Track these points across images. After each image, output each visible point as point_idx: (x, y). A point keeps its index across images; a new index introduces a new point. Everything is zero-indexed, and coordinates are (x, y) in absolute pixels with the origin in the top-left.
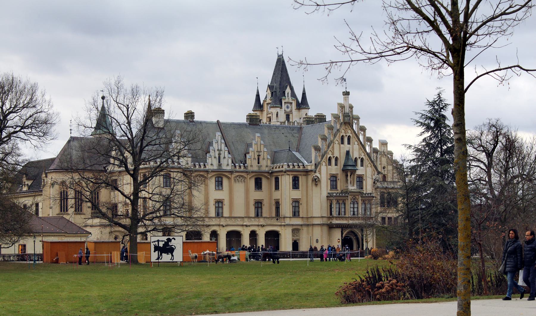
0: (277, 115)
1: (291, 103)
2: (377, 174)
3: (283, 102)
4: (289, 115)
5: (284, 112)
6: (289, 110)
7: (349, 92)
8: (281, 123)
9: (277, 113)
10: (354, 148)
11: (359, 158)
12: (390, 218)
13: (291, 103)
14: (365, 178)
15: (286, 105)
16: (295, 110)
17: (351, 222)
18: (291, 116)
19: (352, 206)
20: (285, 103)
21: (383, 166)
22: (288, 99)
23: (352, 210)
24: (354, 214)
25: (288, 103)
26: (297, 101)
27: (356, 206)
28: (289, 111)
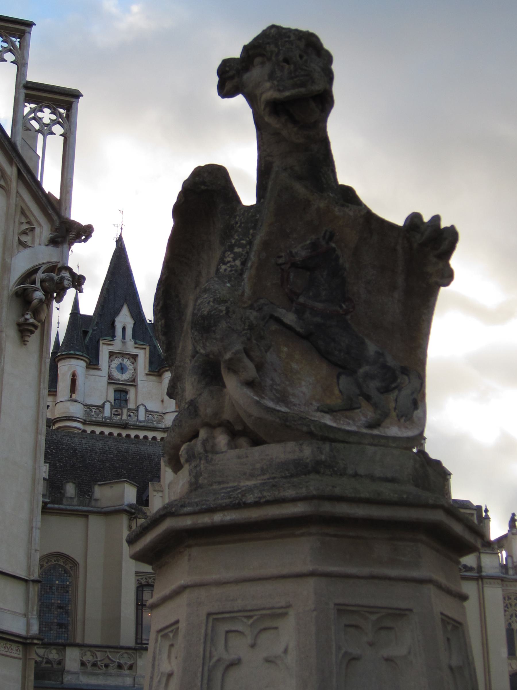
0: (73, 381)
1: (134, 357)
3: (104, 351)
4: (126, 392)
5: (106, 379)
6: (126, 376)
8: (89, 407)
9: (74, 375)
13: (134, 357)
15: (116, 362)
16: (145, 378)
18: (131, 395)
20: (112, 354)
22: (124, 343)
25: (123, 355)
26: (151, 352)
28: (126, 381)
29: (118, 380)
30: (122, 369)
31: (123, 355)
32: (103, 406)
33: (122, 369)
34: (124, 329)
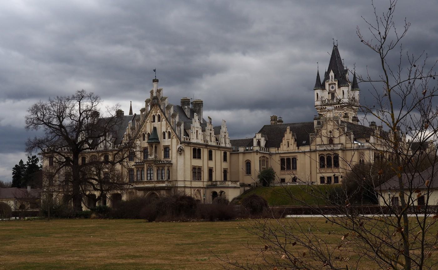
2: (180, 144)
6: (333, 90)
7: (158, 80)
10: (162, 124)
11: (166, 131)
12: (329, 178)
13: (335, 84)
14: (170, 148)
15: (331, 86)
16: (338, 89)
17: (147, 185)
19: (149, 172)
20: (329, 85)
21: (328, 131)
23: (149, 175)
24: (151, 179)
25: (332, 84)
27: (152, 172)
28: (334, 91)
29: (332, 91)
30: (332, 88)
31: (332, 84)
32: (325, 100)
33: (333, 88)
34: (332, 76)
